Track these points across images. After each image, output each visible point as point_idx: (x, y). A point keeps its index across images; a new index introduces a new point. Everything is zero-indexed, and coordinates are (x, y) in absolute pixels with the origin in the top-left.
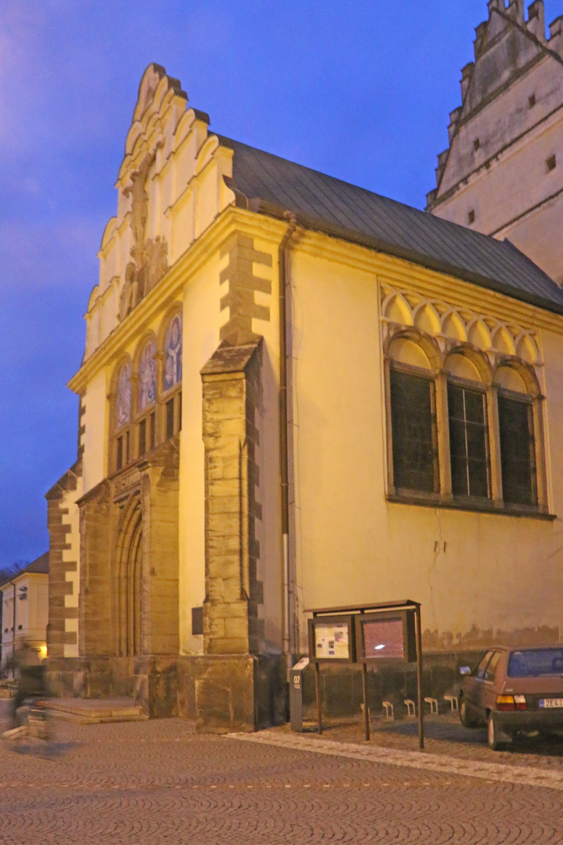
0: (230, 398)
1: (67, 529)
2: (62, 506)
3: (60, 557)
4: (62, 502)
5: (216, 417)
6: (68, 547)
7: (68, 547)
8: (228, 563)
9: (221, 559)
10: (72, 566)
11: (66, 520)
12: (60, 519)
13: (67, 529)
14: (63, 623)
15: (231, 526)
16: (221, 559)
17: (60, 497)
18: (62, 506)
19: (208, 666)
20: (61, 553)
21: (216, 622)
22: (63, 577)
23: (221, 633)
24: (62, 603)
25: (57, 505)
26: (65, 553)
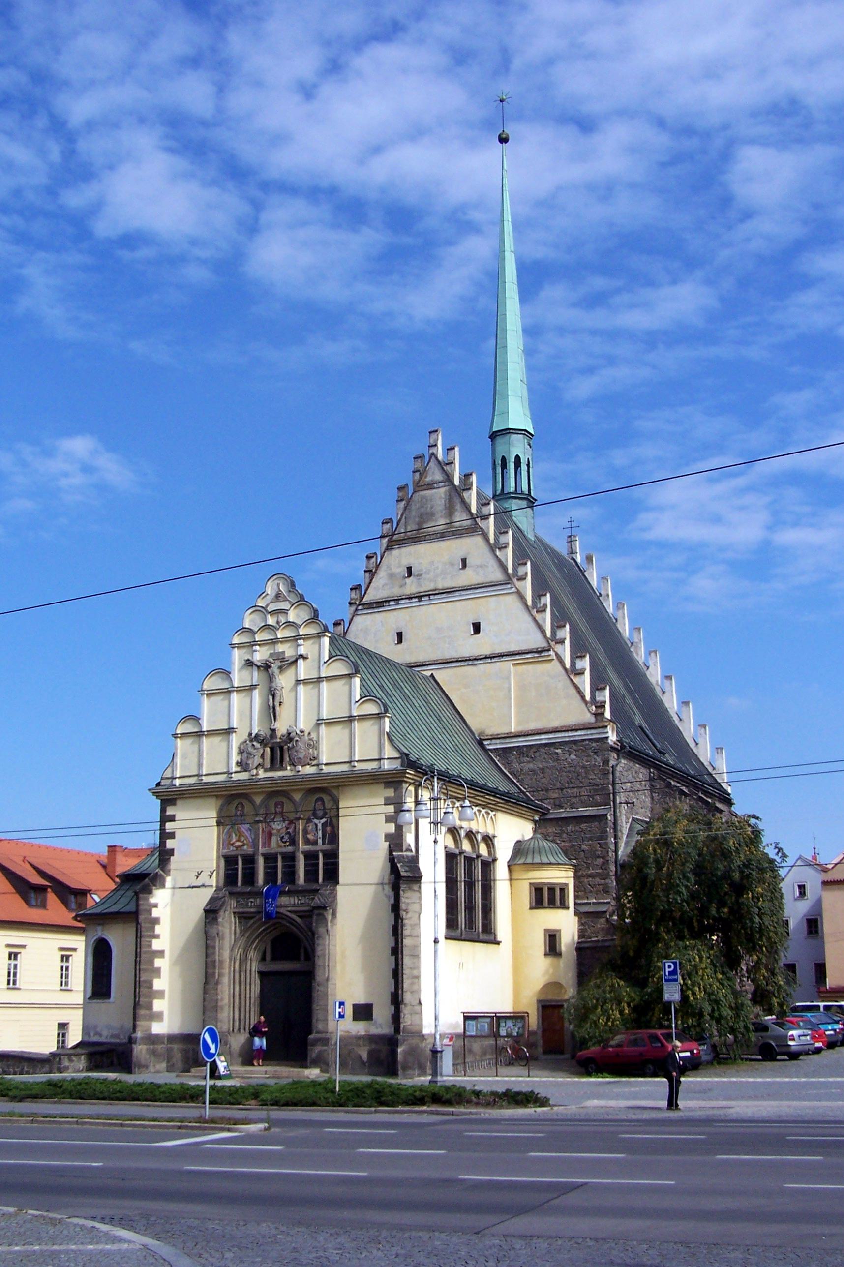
1: (156, 921)
2: (153, 900)
3: (150, 946)
5: (407, 901)
6: (158, 937)
7: (158, 937)
10: (161, 953)
11: (155, 913)
12: (150, 912)
13: (156, 921)
17: (150, 892)
18: (153, 900)
19: (404, 1040)
20: (151, 942)
22: (152, 963)
23: (409, 1023)
25: (147, 899)
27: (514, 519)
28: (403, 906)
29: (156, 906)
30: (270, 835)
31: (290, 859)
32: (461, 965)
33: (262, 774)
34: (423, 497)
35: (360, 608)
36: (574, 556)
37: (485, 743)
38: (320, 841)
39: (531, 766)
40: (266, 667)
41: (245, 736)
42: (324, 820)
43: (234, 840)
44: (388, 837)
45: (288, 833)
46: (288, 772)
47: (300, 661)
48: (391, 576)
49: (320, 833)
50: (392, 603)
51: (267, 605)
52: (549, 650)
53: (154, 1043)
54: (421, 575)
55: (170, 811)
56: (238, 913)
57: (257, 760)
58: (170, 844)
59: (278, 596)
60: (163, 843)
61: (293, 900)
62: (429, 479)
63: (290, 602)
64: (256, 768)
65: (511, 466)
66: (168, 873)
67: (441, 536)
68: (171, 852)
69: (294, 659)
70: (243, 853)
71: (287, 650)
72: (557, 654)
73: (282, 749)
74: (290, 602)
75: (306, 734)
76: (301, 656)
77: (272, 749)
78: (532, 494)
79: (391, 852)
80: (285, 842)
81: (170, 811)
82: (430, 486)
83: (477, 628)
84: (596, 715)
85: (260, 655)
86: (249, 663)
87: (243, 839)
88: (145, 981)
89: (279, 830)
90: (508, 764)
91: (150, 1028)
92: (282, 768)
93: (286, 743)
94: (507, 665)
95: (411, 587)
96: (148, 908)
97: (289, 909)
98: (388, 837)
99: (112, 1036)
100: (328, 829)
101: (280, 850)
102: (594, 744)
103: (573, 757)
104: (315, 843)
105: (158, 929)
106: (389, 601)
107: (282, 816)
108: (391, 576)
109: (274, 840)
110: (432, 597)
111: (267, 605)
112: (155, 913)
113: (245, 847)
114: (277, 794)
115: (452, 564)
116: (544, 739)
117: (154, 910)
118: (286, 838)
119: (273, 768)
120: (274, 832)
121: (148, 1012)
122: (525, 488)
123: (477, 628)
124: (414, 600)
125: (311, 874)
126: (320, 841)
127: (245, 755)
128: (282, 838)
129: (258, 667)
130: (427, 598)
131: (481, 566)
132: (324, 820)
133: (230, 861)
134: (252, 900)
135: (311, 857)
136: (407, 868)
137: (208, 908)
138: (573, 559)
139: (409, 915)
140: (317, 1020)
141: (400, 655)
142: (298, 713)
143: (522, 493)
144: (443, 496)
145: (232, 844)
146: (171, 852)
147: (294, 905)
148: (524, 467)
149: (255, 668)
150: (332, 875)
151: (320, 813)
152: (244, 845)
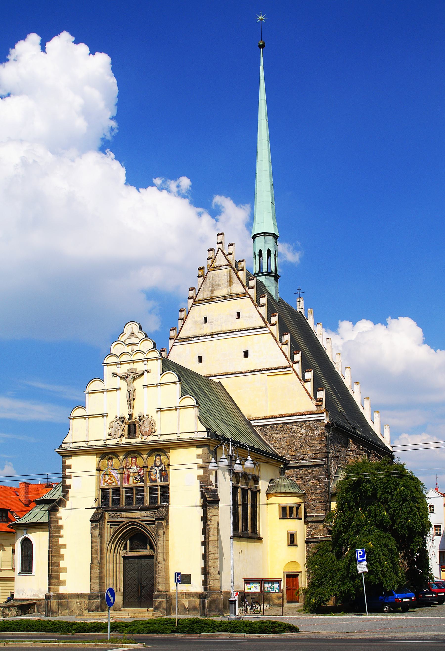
0: (215, 508)
1: (61, 527)
2: (58, 515)
3: (58, 542)
4: (58, 513)
5: (211, 514)
6: (62, 536)
7: (62, 536)
8: (215, 562)
9: (213, 561)
11: (60, 523)
12: (57, 522)
14: (59, 575)
15: (215, 550)
16: (213, 561)
17: (57, 510)
19: (210, 595)
21: (211, 581)
22: (59, 552)
23: (213, 585)
24: (58, 565)
25: (56, 515)
26: (60, 539)
27: (267, 288)
28: (209, 518)
29: (61, 519)
30: (129, 476)
31: (140, 490)
32: (241, 552)
33: (124, 441)
34: (214, 275)
35: (176, 341)
36: (300, 310)
37: (251, 422)
38: (159, 480)
39: (278, 436)
40: (125, 377)
41: (113, 418)
42: (161, 467)
43: (107, 479)
44: (199, 477)
45: (140, 475)
46: (139, 439)
47: (145, 374)
48: (195, 322)
49: (159, 475)
50: (195, 339)
51: (125, 340)
52: (289, 367)
53: (60, 599)
54: (212, 322)
55: (68, 462)
56: (110, 522)
57: (120, 433)
58: (68, 482)
59: (132, 335)
60: (64, 482)
61: (143, 514)
62: (216, 264)
63: (139, 339)
64: (120, 437)
65: (265, 255)
66: (68, 499)
67: (226, 298)
68: (69, 487)
69: (142, 372)
70: (113, 487)
71: (140, 367)
72: (294, 370)
73: (135, 425)
74: (139, 339)
75: (150, 417)
76: (147, 371)
77: (129, 426)
78: (278, 273)
79: (201, 486)
80: (138, 481)
81: (68, 462)
82: (218, 268)
83: (246, 354)
84: (317, 405)
85: (123, 370)
86: (115, 375)
87: (112, 479)
88: (55, 563)
89: (134, 473)
90: (265, 434)
91: (58, 590)
92: (135, 437)
93: (138, 422)
94: (264, 376)
95: (207, 329)
96: (56, 520)
97: (141, 519)
98: (199, 477)
99: (34, 595)
100: (164, 472)
101: (135, 485)
102: (316, 423)
103: (303, 430)
104: (156, 481)
105: (62, 532)
106: (193, 337)
107: (136, 465)
108: (195, 322)
109: (131, 479)
110: (219, 335)
111: (125, 340)
112: (60, 523)
113: (114, 484)
114: (132, 452)
115: (232, 316)
116: (286, 420)
117: (59, 520)
118: (138, 478)
119: (129, 438)
120: (131, 474)
121: (57, 581)
122: (273, 269)
123: (246, 354)
124: (209, 337)
125: (153, 499)
126: (159, 480)
127: (113, 429)
128: (136, 478)
129: (120, 377)
130: (216, 336)
131: (249, 317)
132: (161, 467)
133: (104, 492)
134: (118, 514)
135: (153, 489)
136: (211, 496)
137: (92, 519)
138: (300, 312)
139: (212, 523)
140: (158, 584)
141: (201, 370)
142: (145, 406)
143: (271, 272)
144: (226, 274)
145: (106, 482)
146: (69, 487)
147: (143, 517)
148: (272, 256)
149: (118, 378)
150: (166, 498)
151: (158, 463)
152: (113, 482)
